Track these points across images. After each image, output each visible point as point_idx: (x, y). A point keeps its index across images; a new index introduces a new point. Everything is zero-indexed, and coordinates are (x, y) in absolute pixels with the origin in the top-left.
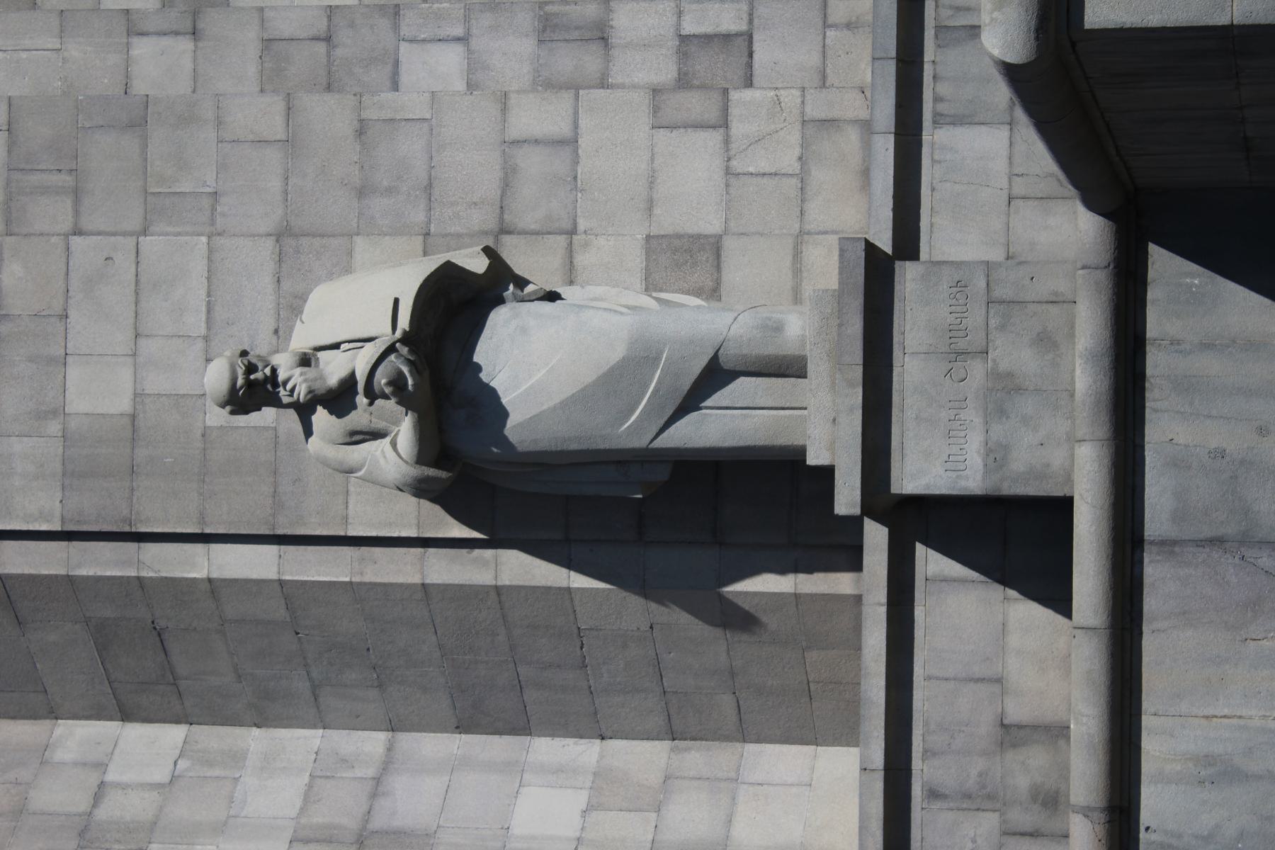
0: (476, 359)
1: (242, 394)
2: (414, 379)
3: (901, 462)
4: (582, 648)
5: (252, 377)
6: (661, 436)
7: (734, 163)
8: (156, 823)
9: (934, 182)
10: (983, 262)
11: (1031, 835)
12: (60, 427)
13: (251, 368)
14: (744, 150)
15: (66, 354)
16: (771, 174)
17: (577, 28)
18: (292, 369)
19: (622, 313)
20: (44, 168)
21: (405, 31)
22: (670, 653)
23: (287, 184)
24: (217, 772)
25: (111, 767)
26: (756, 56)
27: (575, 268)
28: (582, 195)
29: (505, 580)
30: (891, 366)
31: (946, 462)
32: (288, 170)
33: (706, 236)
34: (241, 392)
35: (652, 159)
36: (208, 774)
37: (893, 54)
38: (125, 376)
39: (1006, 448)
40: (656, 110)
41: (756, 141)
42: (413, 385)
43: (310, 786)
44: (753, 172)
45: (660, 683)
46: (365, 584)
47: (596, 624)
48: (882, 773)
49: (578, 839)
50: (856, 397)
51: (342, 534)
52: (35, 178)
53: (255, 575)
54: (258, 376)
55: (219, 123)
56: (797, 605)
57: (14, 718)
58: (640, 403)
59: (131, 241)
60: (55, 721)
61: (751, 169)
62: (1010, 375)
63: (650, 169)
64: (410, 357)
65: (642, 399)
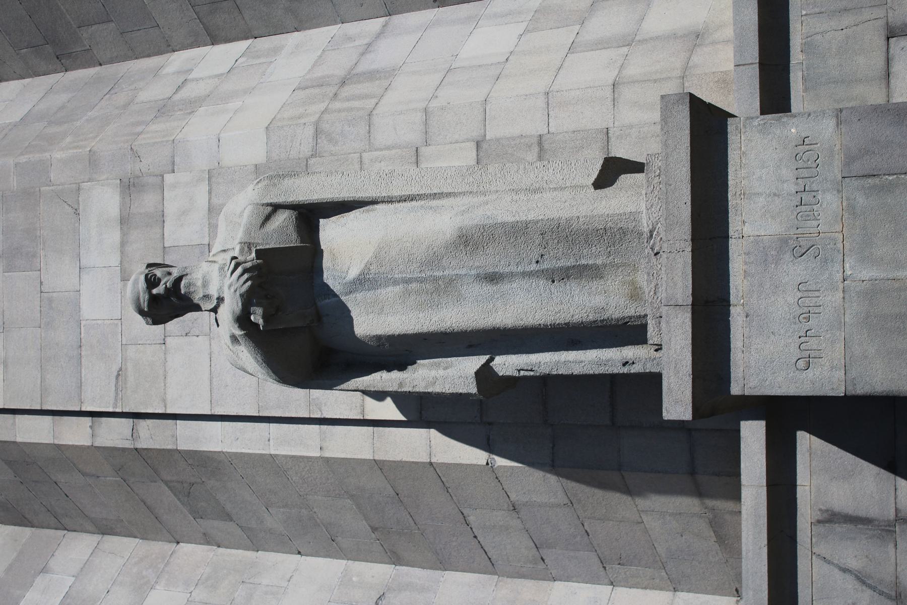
43: (320, 56)
49: (512, 52)
57: (149, 56)
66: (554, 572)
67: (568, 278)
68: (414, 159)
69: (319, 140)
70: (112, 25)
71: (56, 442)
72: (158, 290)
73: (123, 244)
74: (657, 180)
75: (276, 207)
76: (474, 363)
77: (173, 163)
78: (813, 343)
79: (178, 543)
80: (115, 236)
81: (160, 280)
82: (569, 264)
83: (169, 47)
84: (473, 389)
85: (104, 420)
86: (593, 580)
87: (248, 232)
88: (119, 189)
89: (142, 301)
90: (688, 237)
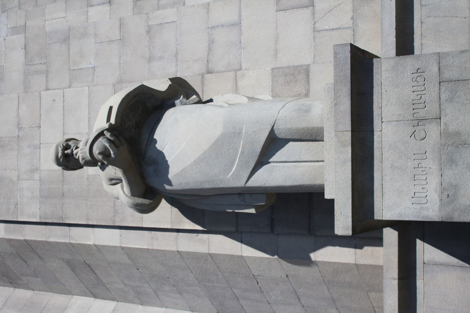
0: (155, 137)
1: (62, 160)
2: (113, 151)
3: (381, 198)
4: (258, 284)
5: (66, 152)
6: (250, 180)
7: (317, 25)
9: (422, 18)
10: (435, 53)
12: (38, 176)
13: (67, 147)
14: (322, 17)
15: (40, 144)
20: (36, 63)
22: (300, 289)
23: (120, 60)
27: (238, 88)
28: (244, 50)
29: (213, 251)
30: (372, 131)
31: (412, 198)
32: (121, 53)
33: (301, 66)
34: (61, 160)
35: (277, 28)
39: (456, 187)
41: (329, 11)
42: (114, 154)
44: (328, 29)
45: (299, 302)
46: (154, 250)
47: (261, 273)
51: (141, 226)
53: (111, 244)
54: (69, 151)
55: (96, 35)
56: (358, 270)
58: (236, 160)
59: (61, 91)
60: (72, 296)
61: (326, 27)
62: (458, 134)
63: (276, 33)
64: (111, 139)
65: (237, 158)
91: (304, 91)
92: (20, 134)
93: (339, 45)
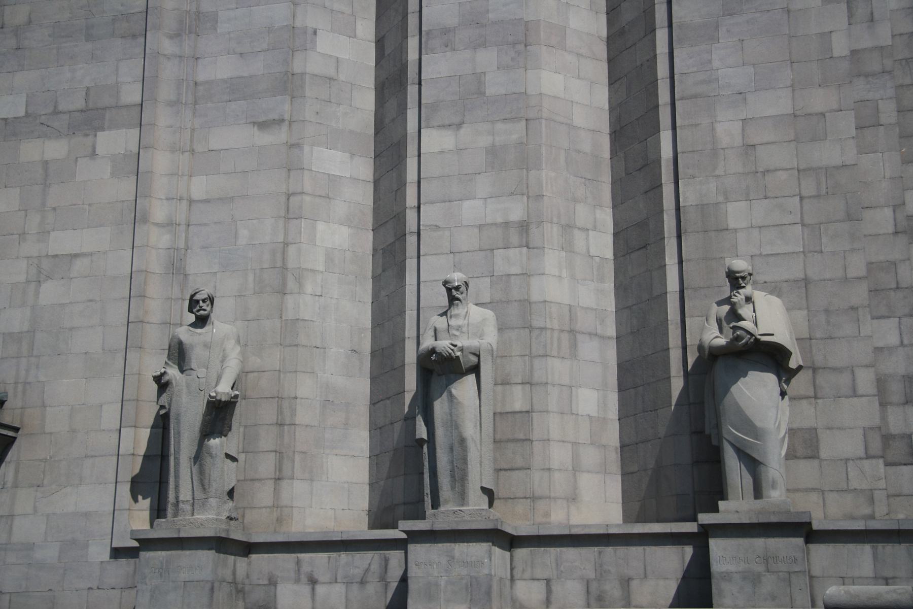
5: (740, 279)
7: (851, 462)
8: (574, 252)
11: (588, 591)
12: (721, 201)
13: (743, 278)
16: (847, 477)
17: (911, 391)
18: (744, 294)
19: (775, 424)
21: (904, 320)
24: (595, 273)
25: (594, 232)
26: (905, 467)
29: (673, 380)
33: (818, 452)
35: (850, 428)
36: (594, 269)
37: (901, 528)
38: (744, 225)
40: (872, 428)
43: (592, 309)
46: (668, 326)
48: (606, 533)
49: (578, 414)
50: (745, 520)
51: (686, 316)
52: (823, 179)
53: (668, 283)
54: (741, 281)
55: (853, 250)
59: (799, 220)
61: (849, 469)
66: (372, 431)
67: (452, 477)
68: (524, 382)
69: (538, 330)
70: (624, 174)
71: (407, 184)
72: (454, 292)
73: (496, 224)
74: (478, 513)
75: (478, 356)
76: (425, 437)
77: (534, 248)
78: (423, 567)
79: (373, 230)
80: (499, 220)
81: (458, 291)
82: (456, 477)
83: (617, 203)
84: (417, 437)
85: (416, 214)
86: (371, 449)
87: (468, 348)
88: (521, 220)
89: (449, 284)
90: (453, 528)
91: (798, 455)
92: (759, 175)
93: (810, 514)
